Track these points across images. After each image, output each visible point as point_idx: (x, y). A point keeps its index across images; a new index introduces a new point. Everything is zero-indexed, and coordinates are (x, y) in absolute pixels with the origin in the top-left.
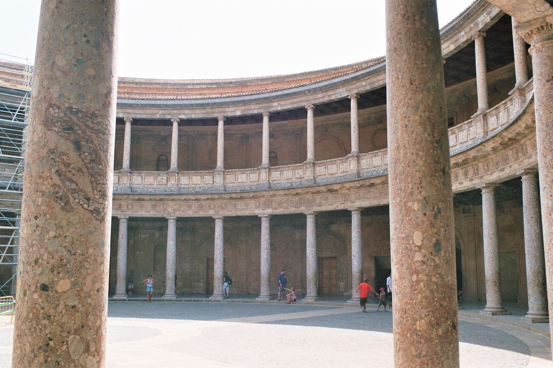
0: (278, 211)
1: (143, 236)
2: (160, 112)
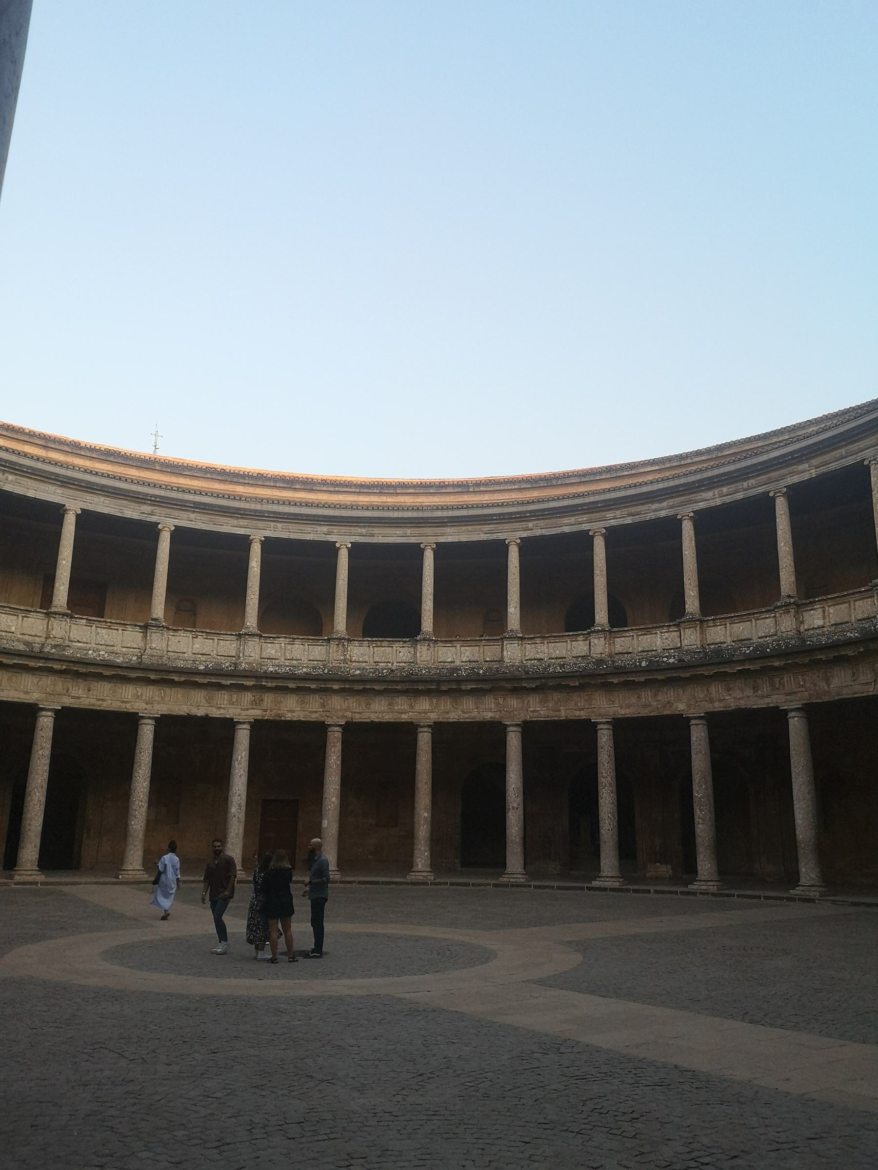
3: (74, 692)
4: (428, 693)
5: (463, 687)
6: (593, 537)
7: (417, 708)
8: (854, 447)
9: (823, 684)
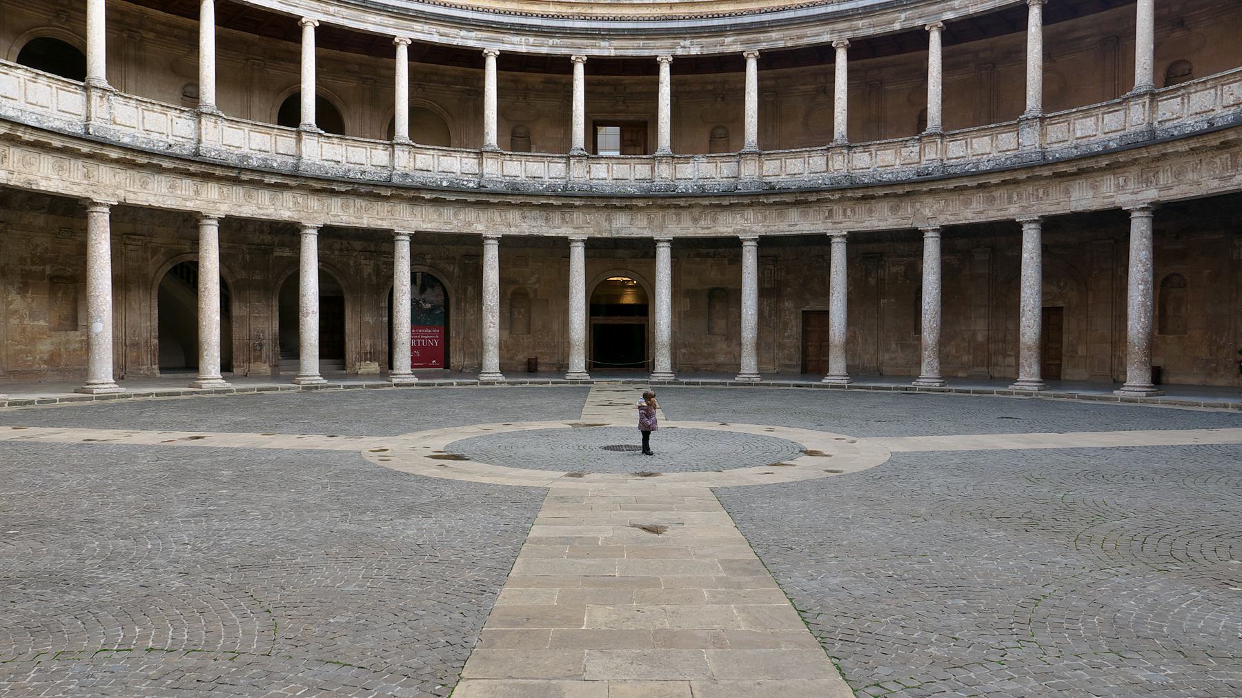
0: (1172, 192)
1: (894, 270)
2: (903, 16)
7: (204, 196)
8: (652, 43)
9: (605, 225)
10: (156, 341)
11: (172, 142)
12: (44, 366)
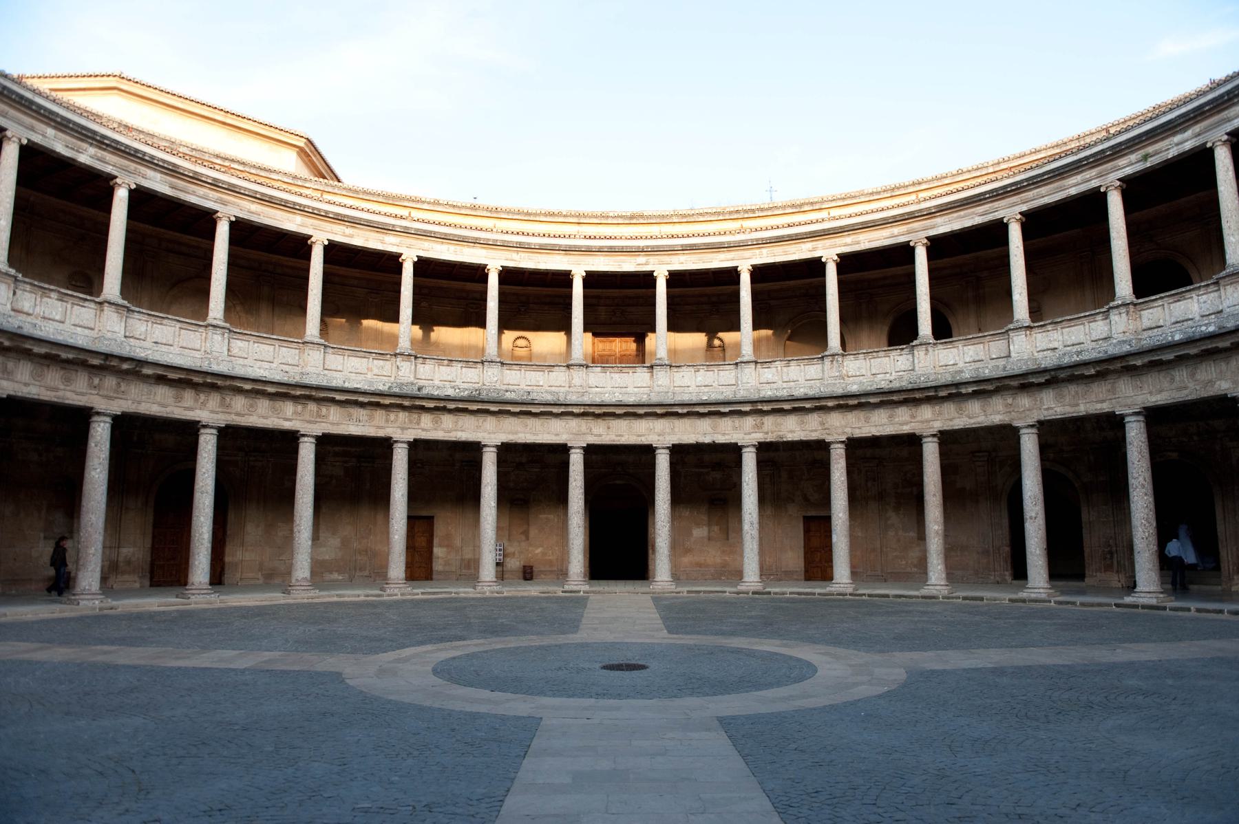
3: (595, 431)
4: (928, 400)
5: (964, 391)
6: (1105, 194)
7: (919, 418)
10: (1007, 549)
11: (892, 378)
12: (915, 570)
